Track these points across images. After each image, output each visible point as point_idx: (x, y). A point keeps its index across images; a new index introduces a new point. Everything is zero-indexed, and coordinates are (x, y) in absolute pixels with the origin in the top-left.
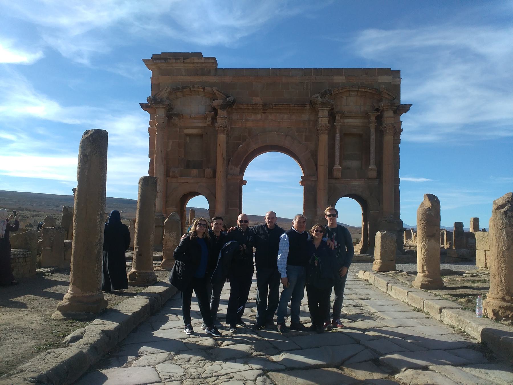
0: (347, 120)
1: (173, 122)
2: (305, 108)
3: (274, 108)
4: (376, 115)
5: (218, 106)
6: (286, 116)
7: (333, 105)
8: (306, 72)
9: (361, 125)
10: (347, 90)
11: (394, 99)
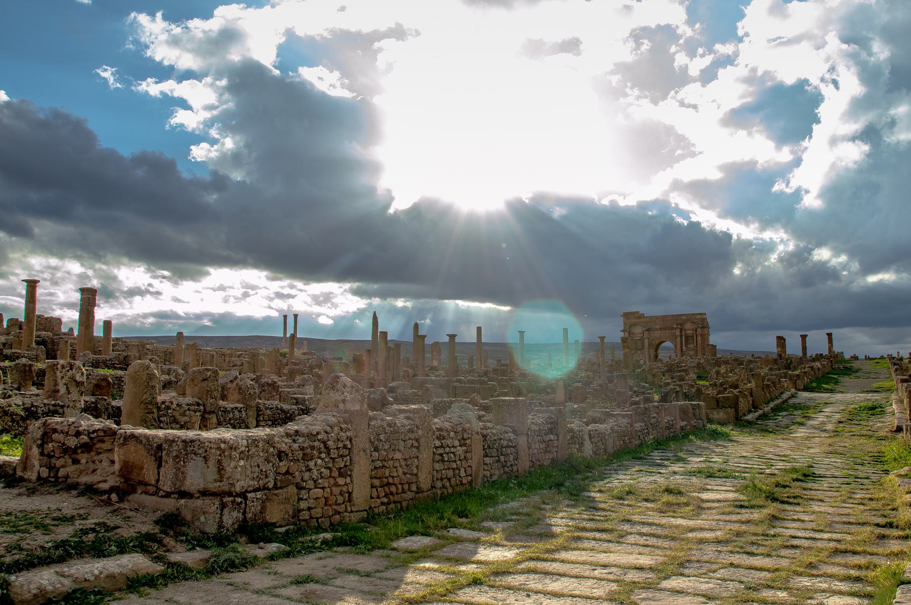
8: (673, 316)
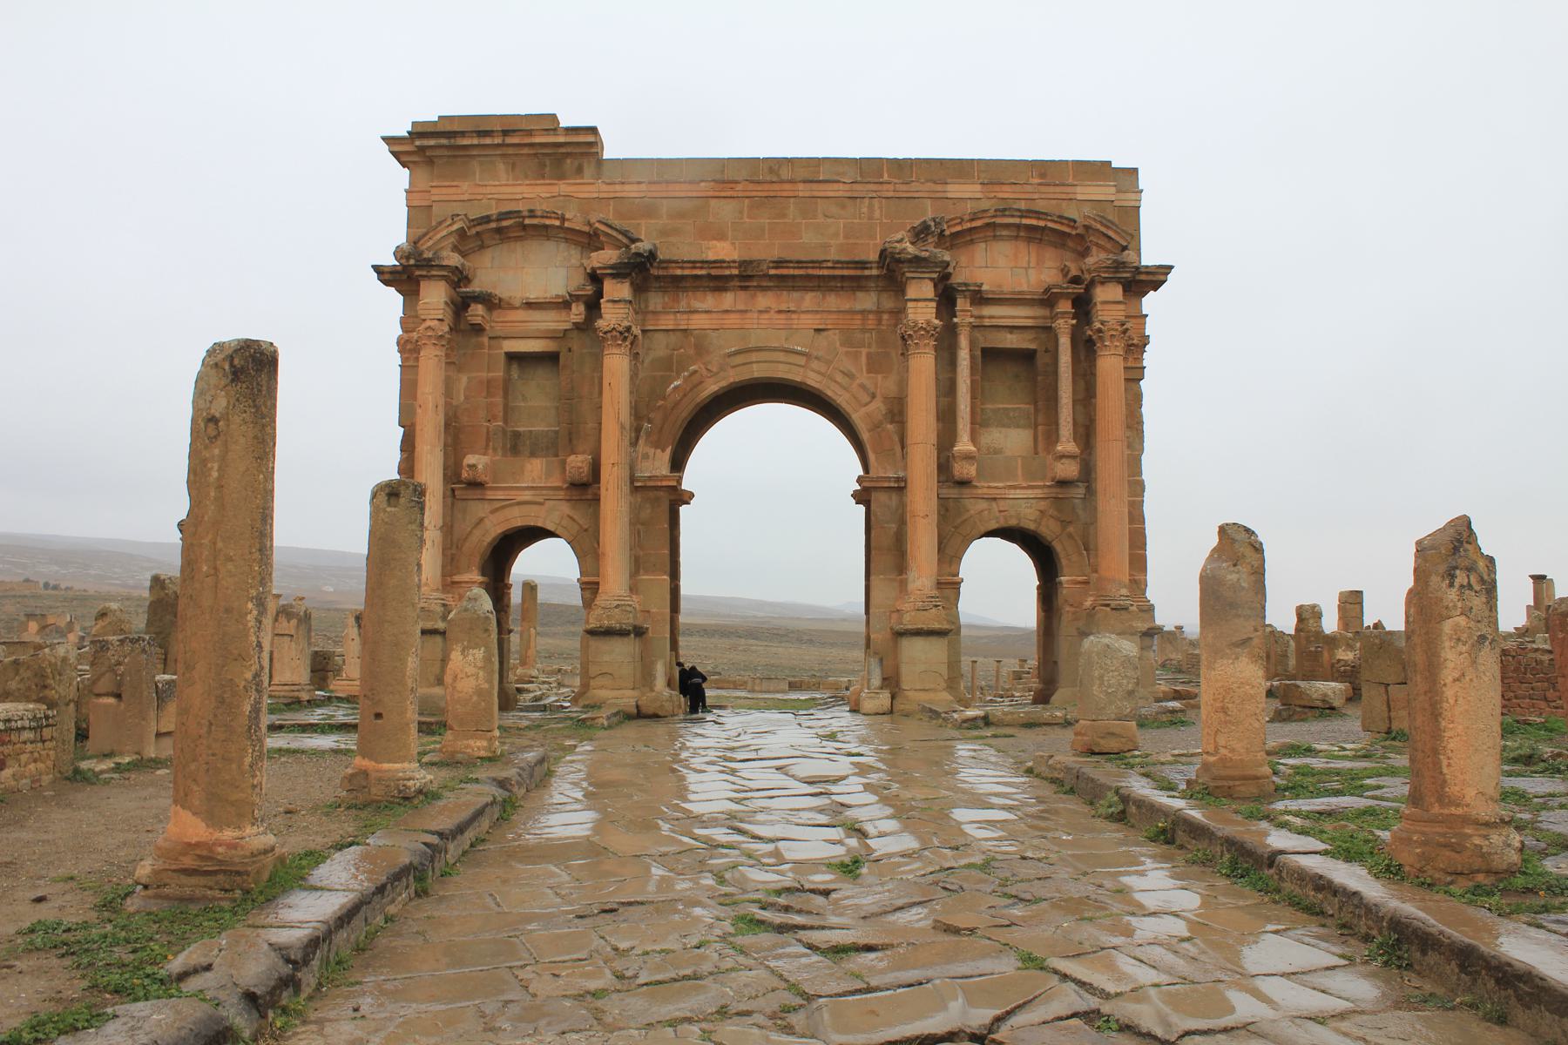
0: (988, 311)
1: (469, 318)
2: (867, 272)
3: (772, 272)
4: (1073, 296)
5: (605, 268)
6: (809, 300)
7: (948, 264)
9: (1030, 323)
10: (987, 221)
11: (1124, 248)
